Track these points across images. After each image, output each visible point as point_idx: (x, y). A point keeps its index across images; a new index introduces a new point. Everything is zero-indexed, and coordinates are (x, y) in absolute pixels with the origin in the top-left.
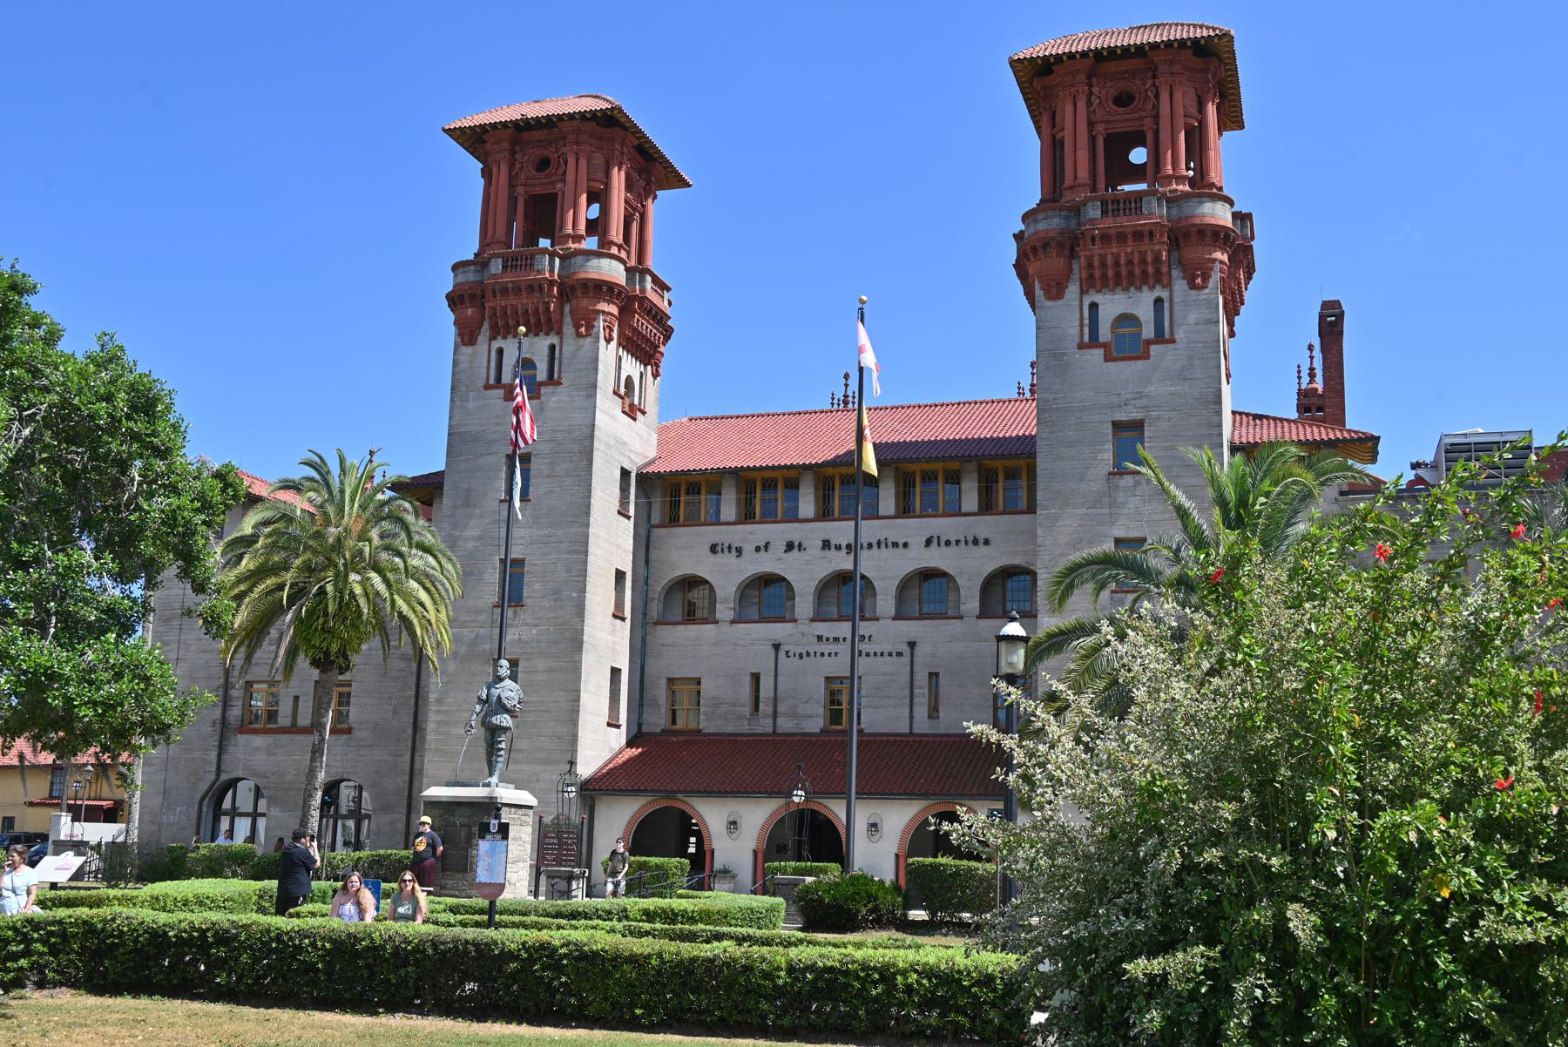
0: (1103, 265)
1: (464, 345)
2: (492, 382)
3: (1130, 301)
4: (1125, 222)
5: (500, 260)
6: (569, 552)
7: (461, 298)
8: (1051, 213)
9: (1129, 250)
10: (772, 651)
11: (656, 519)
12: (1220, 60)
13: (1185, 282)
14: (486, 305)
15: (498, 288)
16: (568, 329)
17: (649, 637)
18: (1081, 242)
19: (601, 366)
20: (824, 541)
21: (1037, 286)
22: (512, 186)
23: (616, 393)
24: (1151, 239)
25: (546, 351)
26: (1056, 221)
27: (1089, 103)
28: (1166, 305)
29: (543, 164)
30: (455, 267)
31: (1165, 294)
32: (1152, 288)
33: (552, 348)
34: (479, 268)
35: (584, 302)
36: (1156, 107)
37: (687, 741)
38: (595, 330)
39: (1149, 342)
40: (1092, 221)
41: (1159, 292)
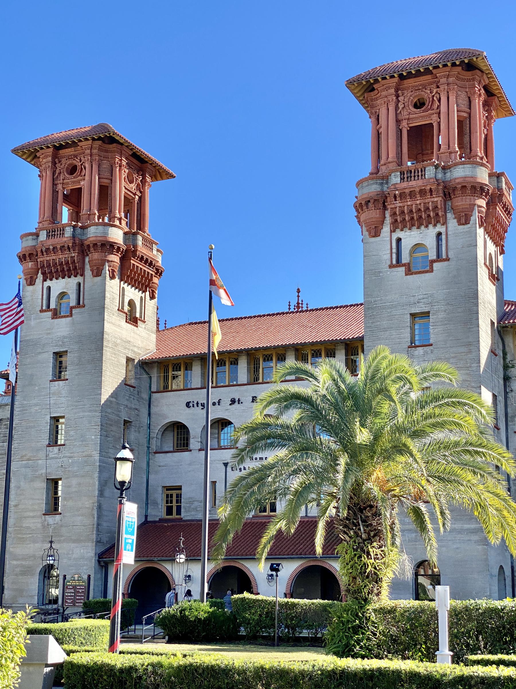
0: (403, 212)
1: (28, 285)
2: (44, 308)
3: (421, 236)
4: (415, 184)
5: (45, 231)
6: (90, 411)
7: (24, 255)
8: (371, 182)
9: (418, 202)
10: (224, 467)
11: (154, 389)
12: (482, 72)
13: (455, 220)
14: (39, 260)
15: (44, 249)
16: (88, 272)
17: (151, 461)
18: (388, 199)
19: (107, 295)
20: (253, 397)
22: (54, 185)
23: (121, 310)
24: (431, 195)
25: (75, 287)
26: (374, 186)
27: (397, 108)
28: (444, 237)
29: (73, 170)
30: (22, 237)
31: (442, 229)
32: (435, 225)
33: (79, 284)
34: (35, 237)
35: (96, 256)
36: (439, 107)
37: (173, 525)
38: (103, 272)
39: (432, 262)
40: (395, 184)
41: (440, 228)
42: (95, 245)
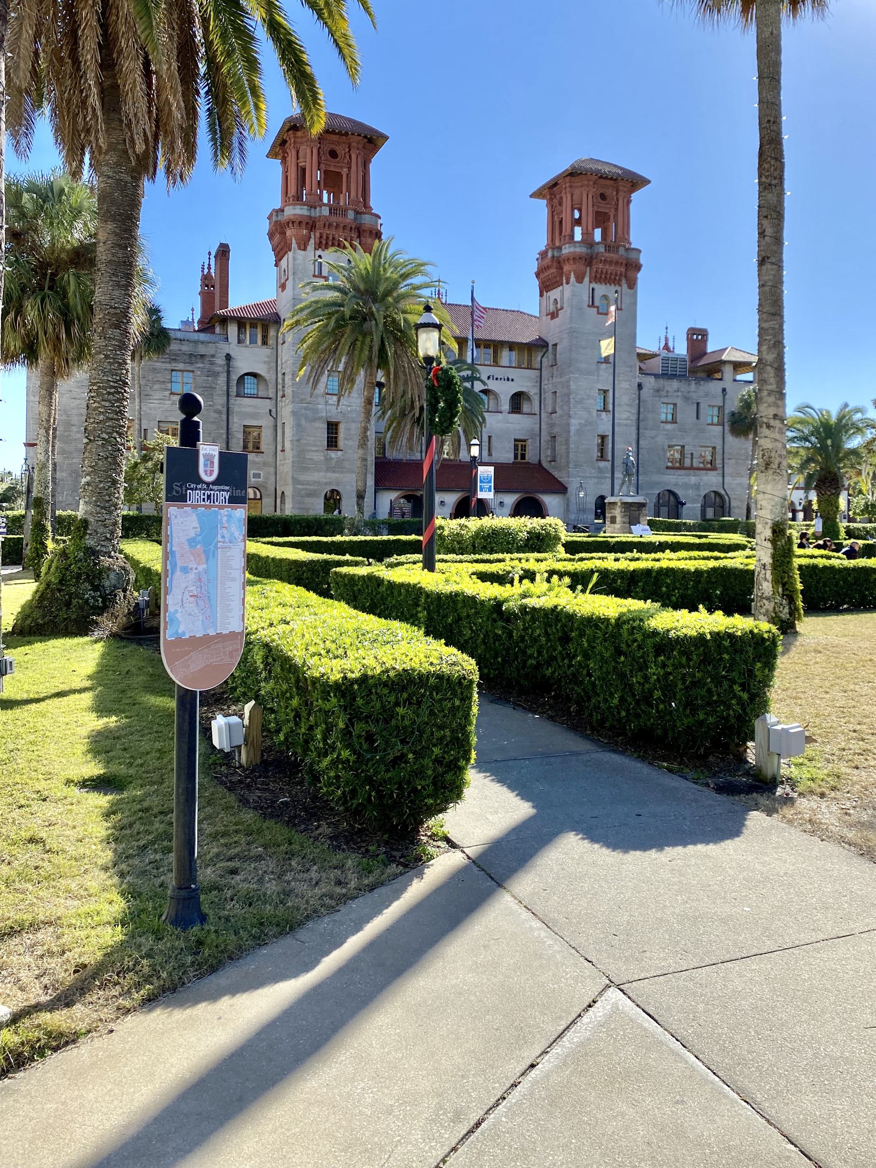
1: (300, 249)
21: (572, 275)
35: (369, 240)
41: (617, 288)
42: (371, 232)
